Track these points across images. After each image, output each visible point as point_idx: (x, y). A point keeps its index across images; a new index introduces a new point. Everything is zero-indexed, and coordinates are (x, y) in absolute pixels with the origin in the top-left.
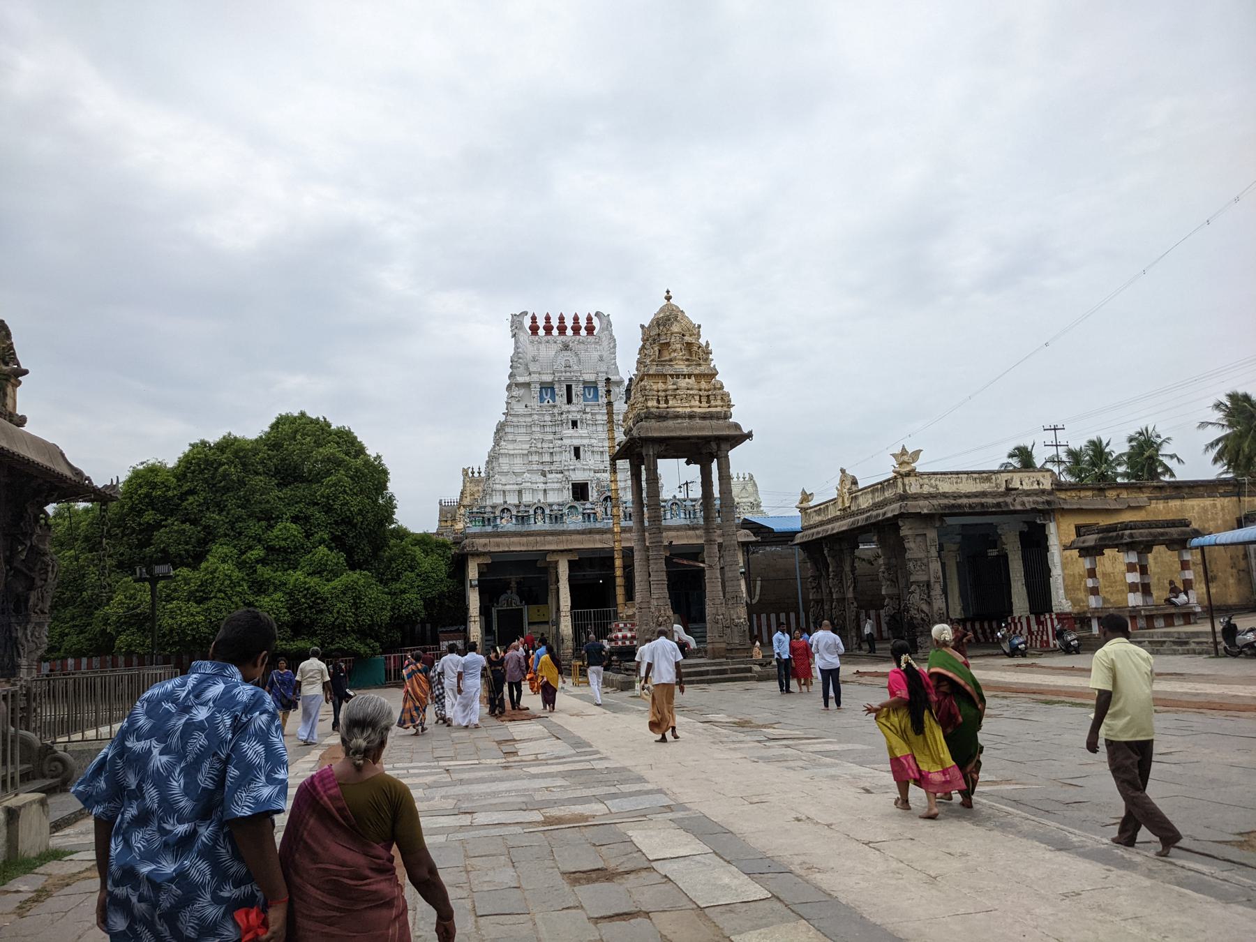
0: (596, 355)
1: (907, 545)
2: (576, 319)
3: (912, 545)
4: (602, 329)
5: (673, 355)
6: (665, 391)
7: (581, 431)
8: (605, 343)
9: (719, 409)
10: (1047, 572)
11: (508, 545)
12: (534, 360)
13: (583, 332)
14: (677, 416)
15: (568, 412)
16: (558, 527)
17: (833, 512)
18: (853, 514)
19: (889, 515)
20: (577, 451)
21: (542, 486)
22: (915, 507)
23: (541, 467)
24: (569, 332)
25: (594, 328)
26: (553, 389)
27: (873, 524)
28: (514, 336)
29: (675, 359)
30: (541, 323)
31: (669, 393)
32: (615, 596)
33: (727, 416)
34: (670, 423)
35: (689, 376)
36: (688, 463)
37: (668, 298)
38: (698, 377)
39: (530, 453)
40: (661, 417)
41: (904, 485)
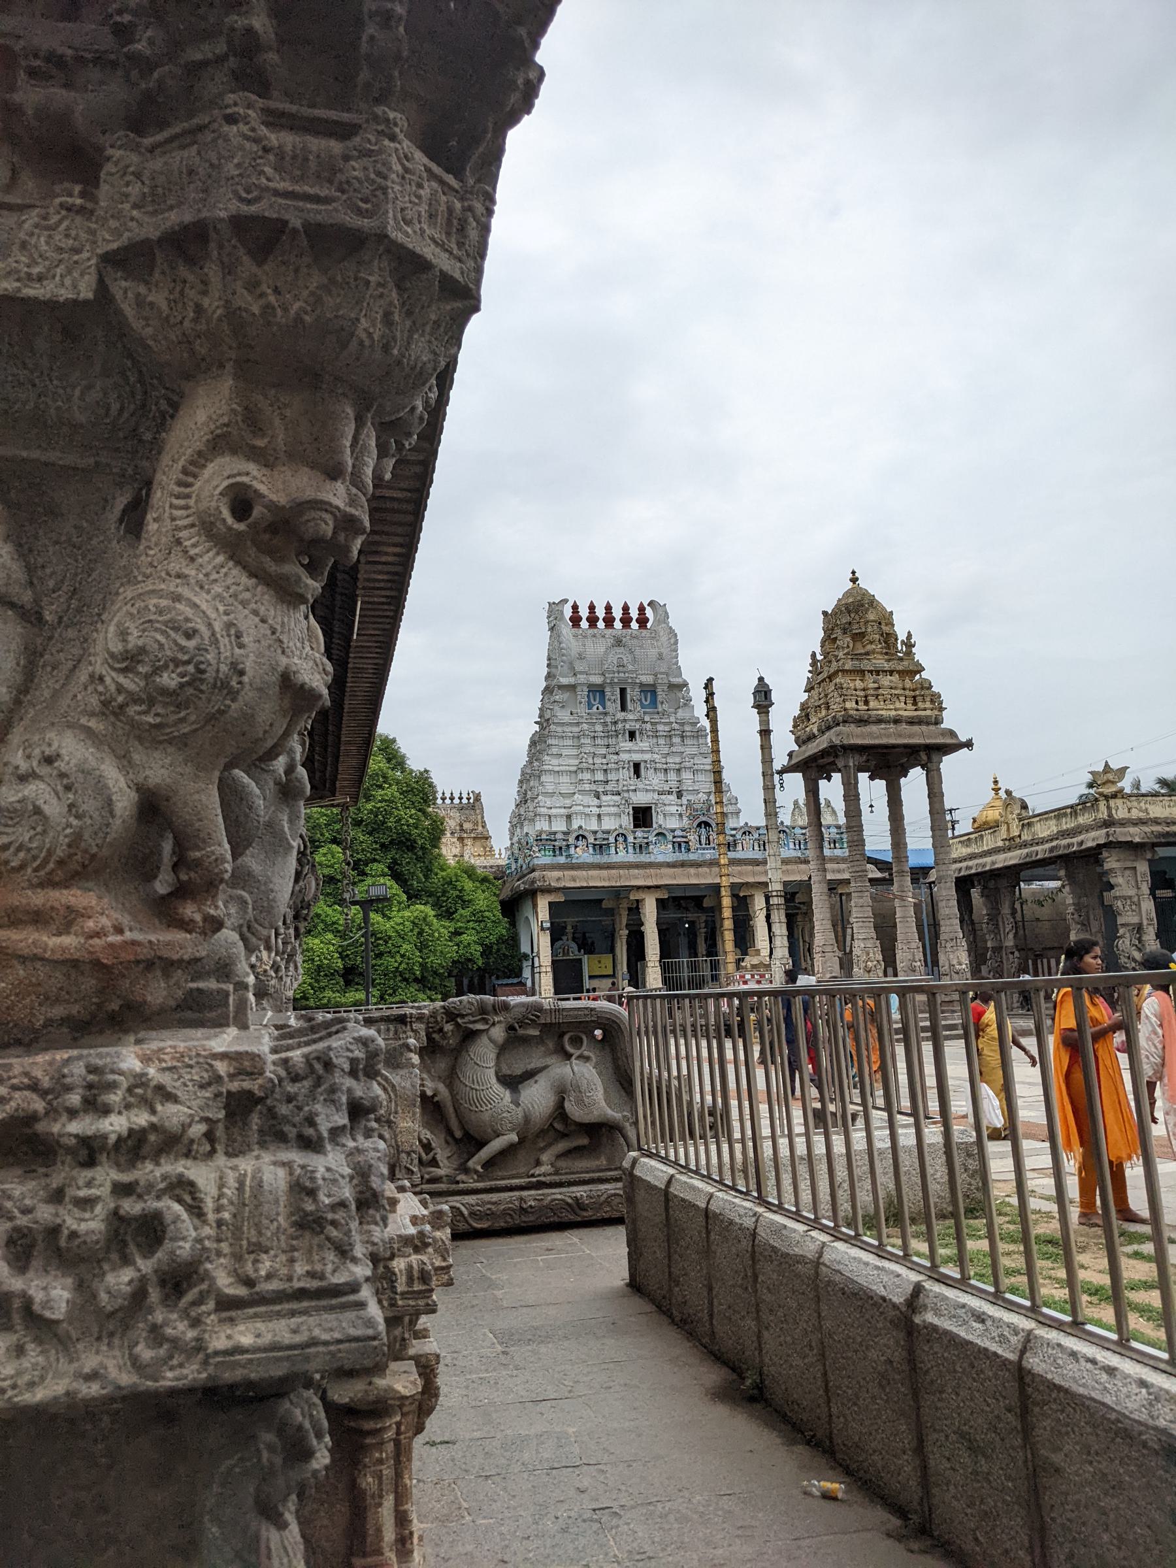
0: (653, 653)
1: (1112, 881)
2: (626, 608)
3: (1120, 880)
4: (658, 621)
5: (869, 647)
6: (864, 690)
7: (643, 744)
8: (664, 639)
9: (928, 713)
11: (587, 879)
12: (581, 657)
13: (634, 625)
14: (880, 721)
15: (625, 721)
16: (643, 858)
17: (989, 842)
18: (1025, 845)
19: (1090, 844)
20: (637, 767)
21: (595, 810)
22: (1125, 834)
23: (594, 787)
24: (618, 625)
25: (648, 620)
26: (602, 693)
27: (1060, 857)
28: (552, 629)
29: (874, 652)
30: (584, 613)
31: (869, 692)
33: (938, 721)
34: (874, 728)
35: (891, 673)
36: (872, 778)
37: (854, 580)
38: (903, 673)
39: (582, 770)
40: (862, 722)
41: (1109, 808)
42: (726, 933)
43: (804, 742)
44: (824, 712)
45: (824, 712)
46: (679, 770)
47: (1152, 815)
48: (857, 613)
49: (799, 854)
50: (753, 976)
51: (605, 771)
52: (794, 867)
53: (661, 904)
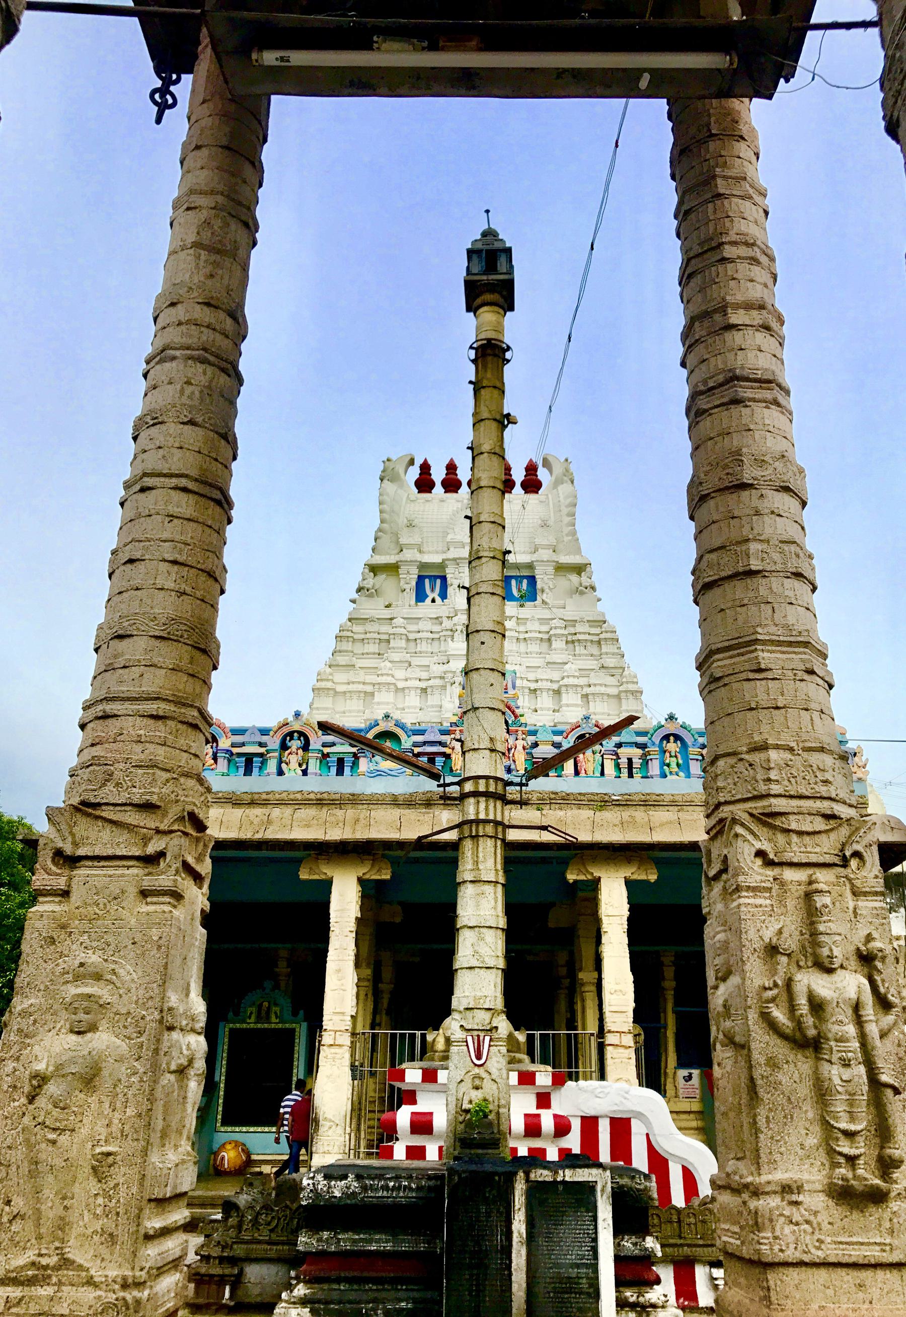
30: (438, 474)
46: (558, 692)
51: (424, 690)
53: (371, 892)
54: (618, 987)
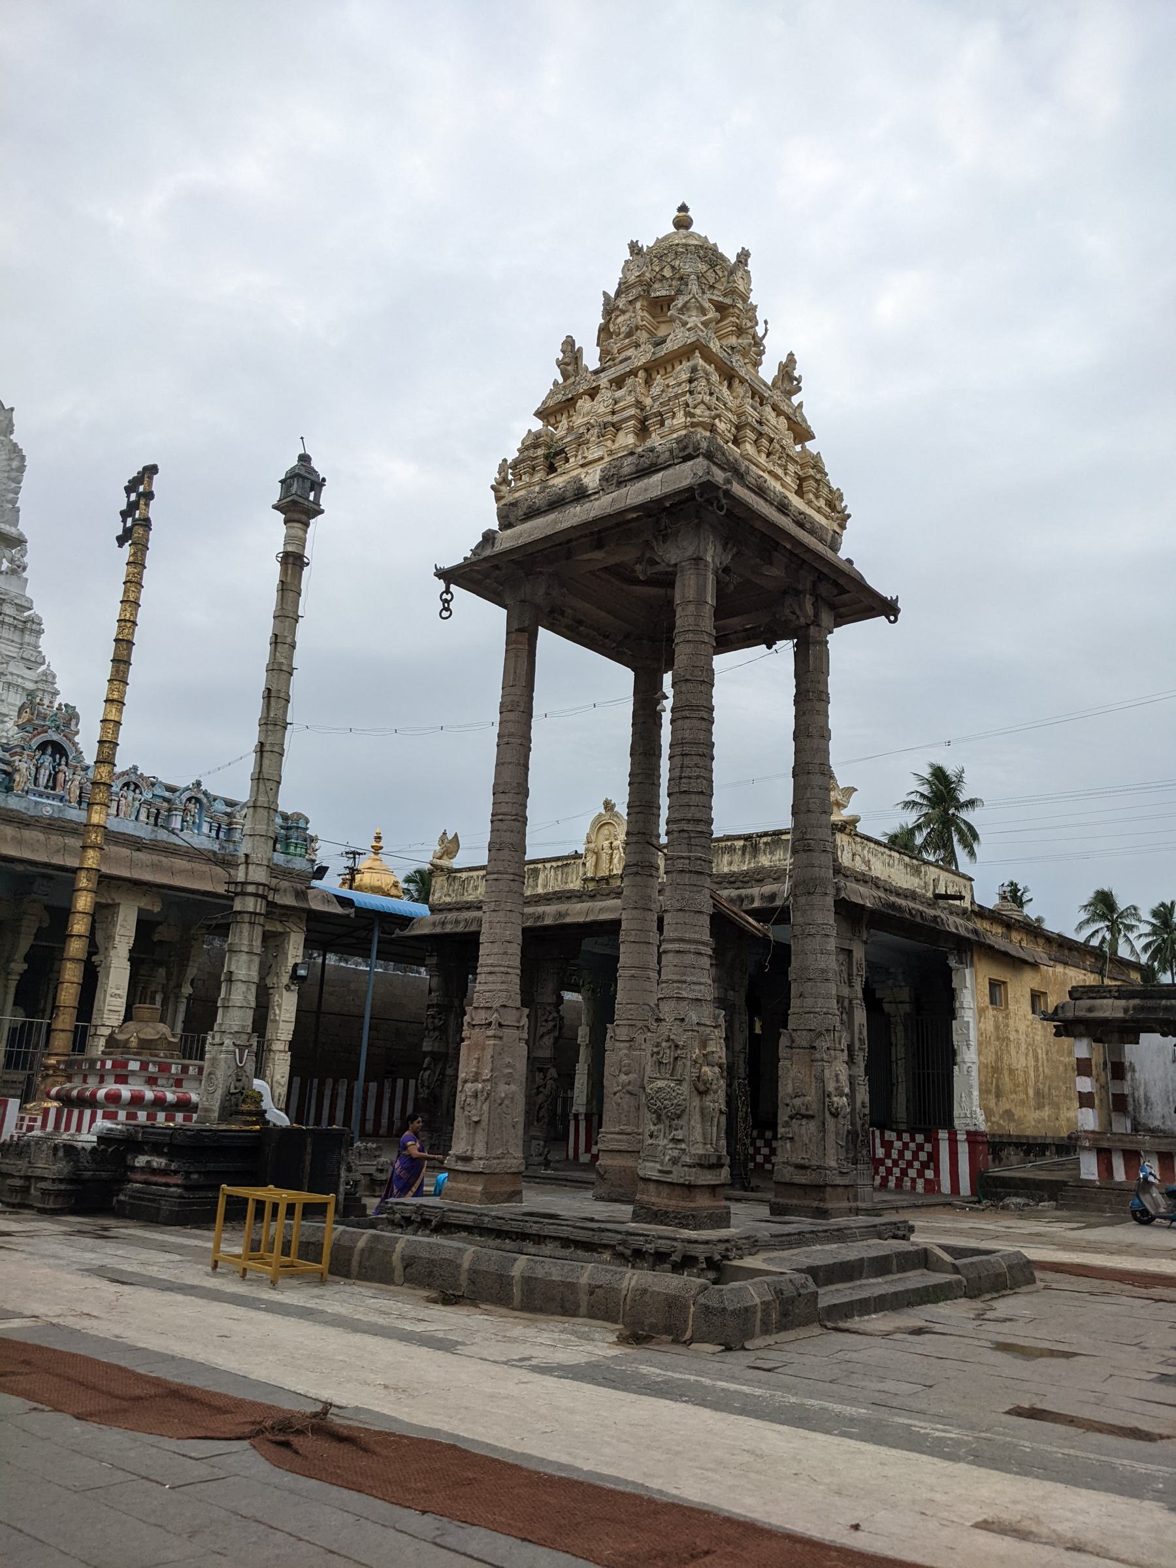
10: (949, 1056)
22: (855, 892)
32: (58, 983)
42: (69, 965)
43: (533, 513)
44: (627, 439)
45: (627, 439)
47: (874, 873)
48: (712, 266)
49: (216, 847)
50: (144, 1066)
52: (205, 868)
54: (118, 992)
